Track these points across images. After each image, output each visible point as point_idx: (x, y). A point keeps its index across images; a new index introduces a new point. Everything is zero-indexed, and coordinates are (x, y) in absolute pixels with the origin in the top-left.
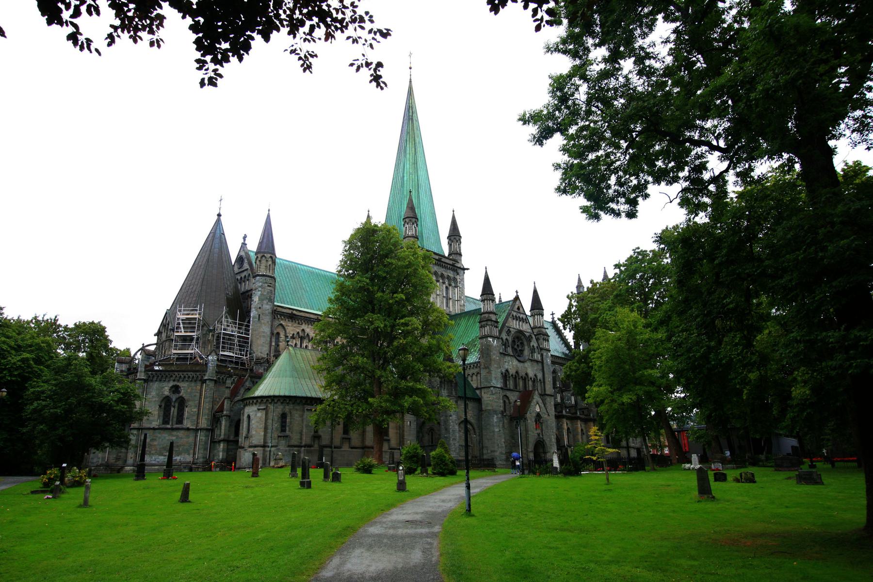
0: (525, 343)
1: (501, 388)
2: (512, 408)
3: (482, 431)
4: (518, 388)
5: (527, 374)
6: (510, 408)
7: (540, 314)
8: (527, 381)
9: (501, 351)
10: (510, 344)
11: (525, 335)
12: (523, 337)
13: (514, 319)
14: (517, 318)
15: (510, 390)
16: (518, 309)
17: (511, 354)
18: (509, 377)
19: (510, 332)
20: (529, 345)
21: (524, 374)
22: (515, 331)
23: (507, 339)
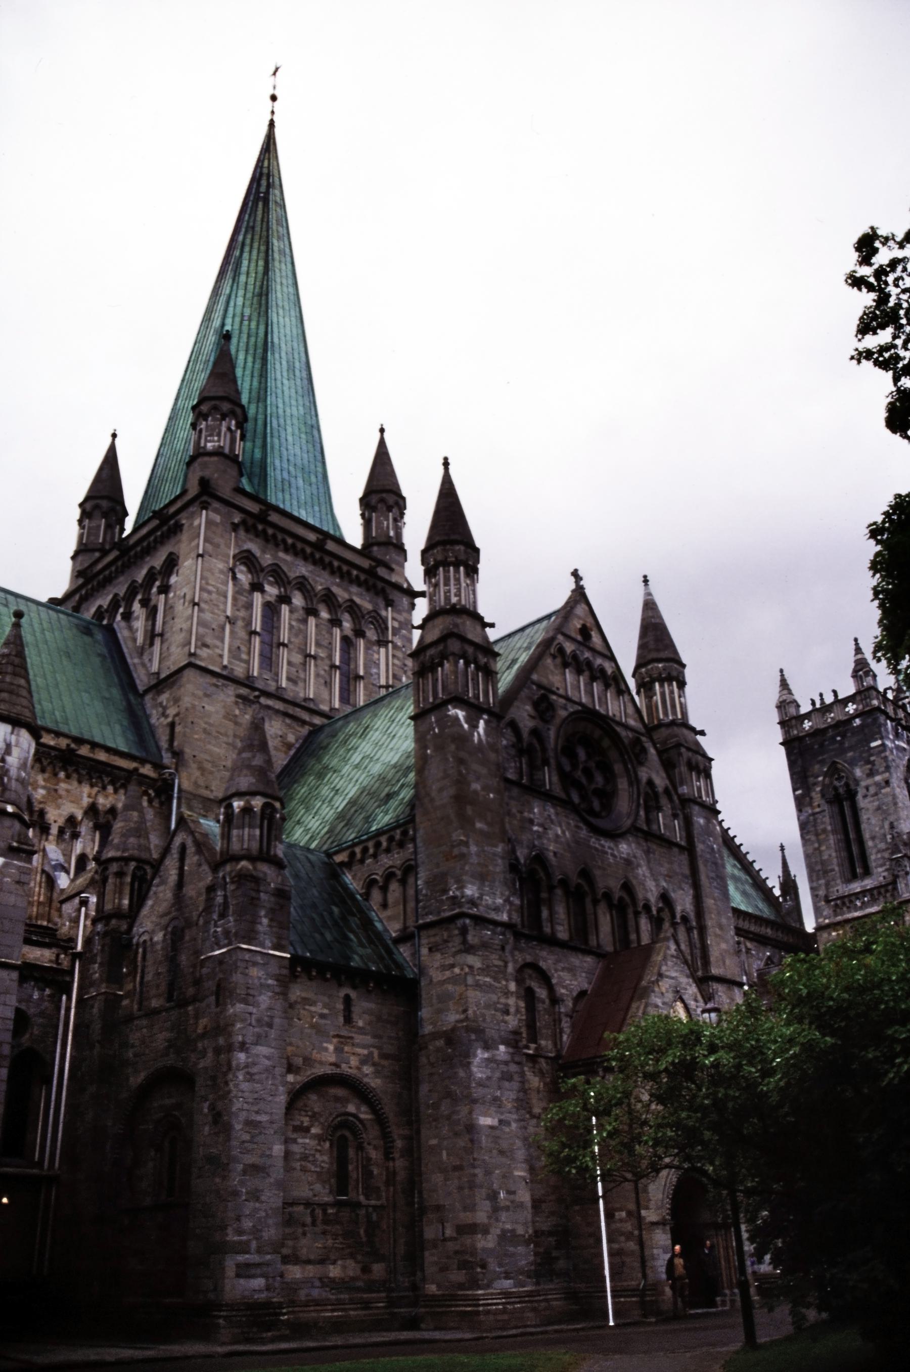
0: (618, 768)
1: (508, 926)
2: (566, 1024)
3: (418, 1132)
4: (593, 942)
5: (627, 887)
6: (557, 1021)
7: (670, 679)
8: (631, 916)
9: (511, 775)
10: (551, 754)
11: (615, 738)
12: (606, 743)
13: (565, 665)
14: (579, 666)
15: (552, 942)
16: (585, 632)
17: (558, 791)
18: (551, 889)
19: (551, 707)
20: (634, 780)
21: (615, 885)
22: (572, 708)
23: (534, 732)
